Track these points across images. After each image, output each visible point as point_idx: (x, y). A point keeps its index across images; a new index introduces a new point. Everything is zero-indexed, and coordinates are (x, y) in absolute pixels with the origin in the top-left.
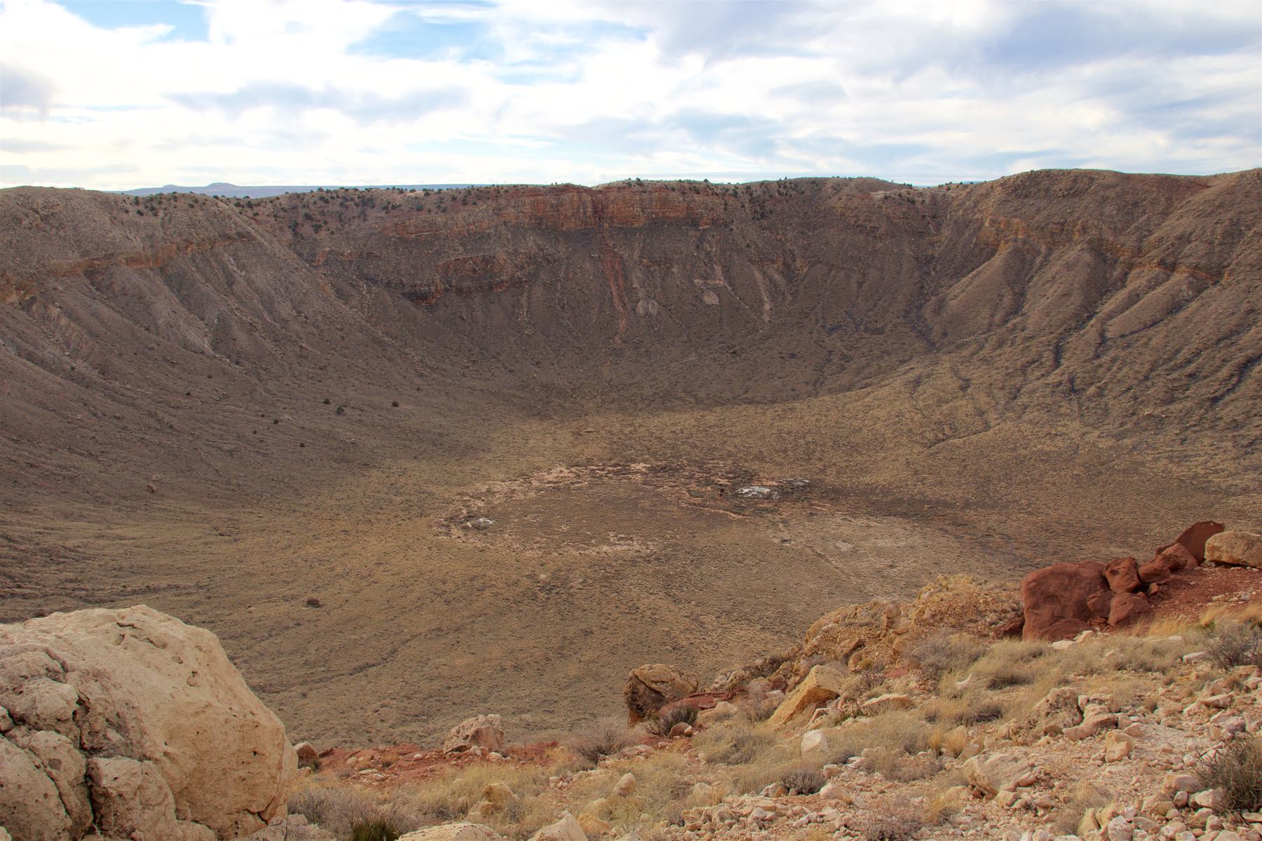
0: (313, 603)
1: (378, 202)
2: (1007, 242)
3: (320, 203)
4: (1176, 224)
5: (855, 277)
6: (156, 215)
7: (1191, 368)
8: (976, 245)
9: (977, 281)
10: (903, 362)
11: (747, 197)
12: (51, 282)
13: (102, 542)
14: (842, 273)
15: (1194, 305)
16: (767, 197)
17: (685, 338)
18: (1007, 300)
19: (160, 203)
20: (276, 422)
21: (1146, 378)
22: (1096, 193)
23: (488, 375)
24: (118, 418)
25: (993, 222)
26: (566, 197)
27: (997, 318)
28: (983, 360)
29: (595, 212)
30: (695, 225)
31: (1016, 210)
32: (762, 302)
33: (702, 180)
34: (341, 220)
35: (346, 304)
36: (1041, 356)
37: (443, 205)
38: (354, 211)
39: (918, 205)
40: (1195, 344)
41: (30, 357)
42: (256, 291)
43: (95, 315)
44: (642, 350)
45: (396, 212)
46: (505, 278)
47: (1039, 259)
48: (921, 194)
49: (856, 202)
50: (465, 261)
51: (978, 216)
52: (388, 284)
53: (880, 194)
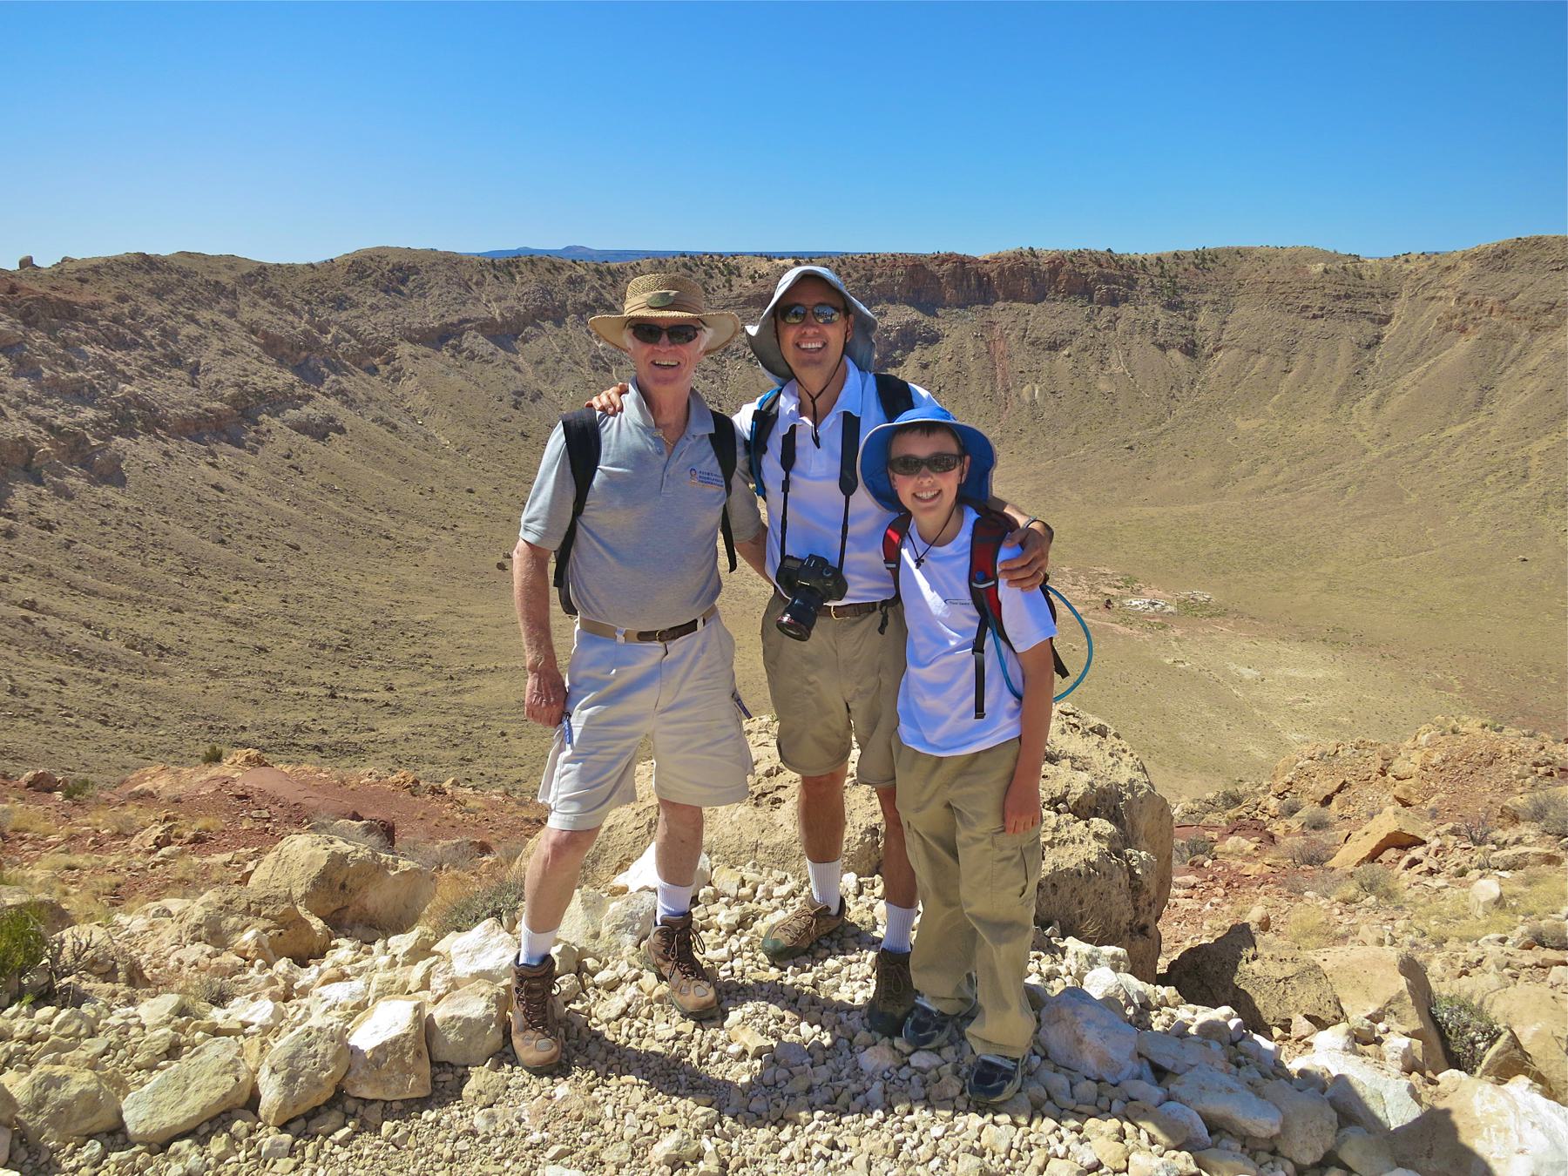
2: (1476, 326)
5: (1280, 364)
9: (1432, 373)
11: (1158, 270)
12: (404, 349)
13: (452, 618)
16: (1180, 269)
18: (1471, 395)
24: (470, 491)
33: (1103, 249)
38: (720, 280)
39: (1367, 282)
47: (1516, 348)
51: (1442, 293)
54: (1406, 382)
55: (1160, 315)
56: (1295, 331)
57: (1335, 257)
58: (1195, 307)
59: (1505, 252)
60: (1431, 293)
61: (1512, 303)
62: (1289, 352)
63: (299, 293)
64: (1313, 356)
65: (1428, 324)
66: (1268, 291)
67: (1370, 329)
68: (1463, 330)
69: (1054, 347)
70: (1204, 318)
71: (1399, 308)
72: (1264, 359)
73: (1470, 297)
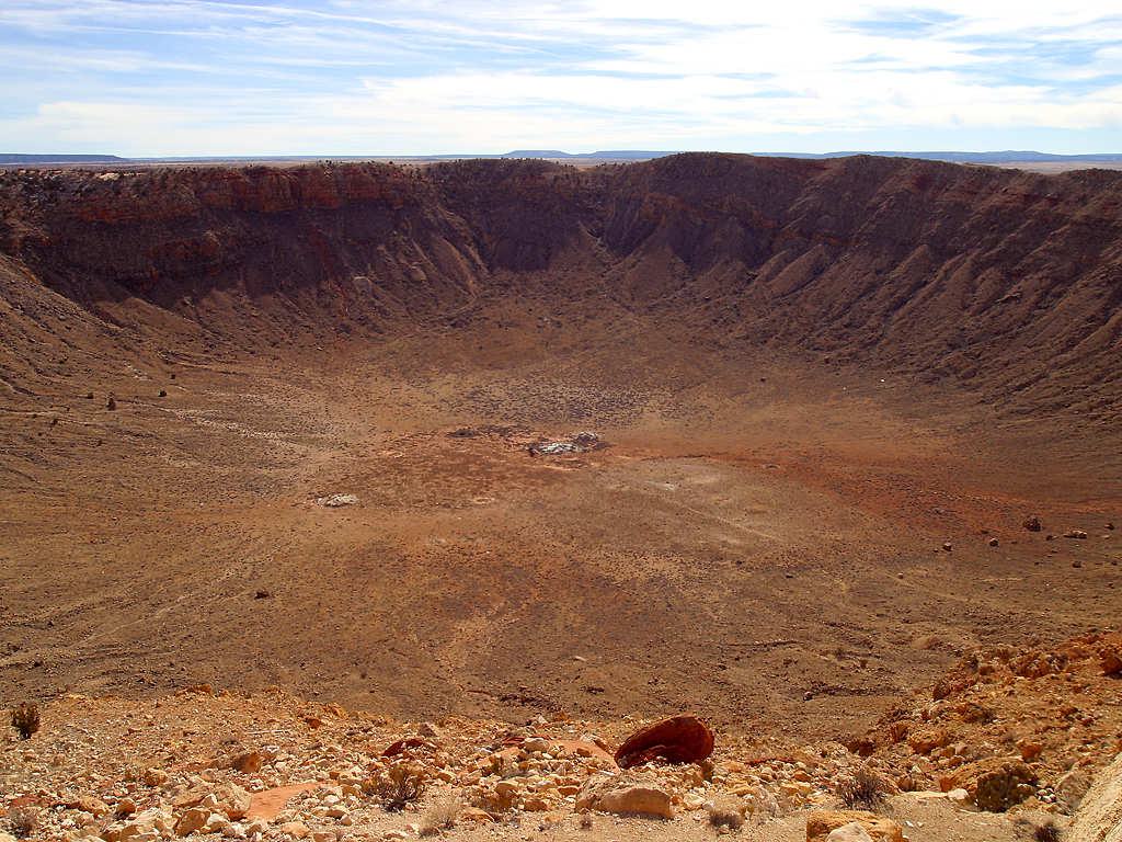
0: (261, 595)
4: (808, 199)
7: (846, 320)
8: (639, 219)
14: (529, 248)
15: (834, 268)
21: (813, 330)
23: (231, 358)
25: (652, 198)
30: (390, 206)
32: (465, 278)
40: (843, 299)
46: (218, 261)
48: (583, 175)
50: (175, 245)
52: (98, 272)
53: (550, 176)
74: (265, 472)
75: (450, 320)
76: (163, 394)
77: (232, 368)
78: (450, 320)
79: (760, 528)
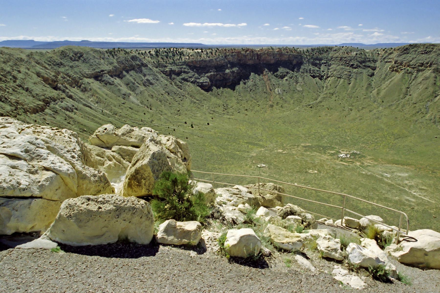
1: (185, 53)
2: (402, 70)
3: (165, 54)
6: (114, 57)
9: (392, 83)
10: (370, 111)
12: (86, 80)
17: (292, 102)
18: (404, 90)
19: (114, 52)
20: (174, 130)
22: (435, 52)
26: (248, 52)
27: (401, 96)
28: (399, 111)
29: (258, 58)
31: (404, 58)
34: (173, 60)
35: (179, 88)
36: (421, 110)
37: (208, 55)
41: (89, 107)
42: (151, 84)
43: (103, 92)
44: (280, 105)
45: (192, 57)
47: (414, 76)
49: (346, 55)
51: (389, 60)
54: (384, 86)
55: (311, 67)
56: (350, 72)
57: (357, 50)
58: (320, 65)
59: (407, 49)
60: (386, 60)
61: (411, 63)
62: (349, 77)
63: (46, 61)
64: (356, 79)
65: (387, 69)
66: (341, 60)
67: (371, 71)
68: (396, 71)
69: (282, 77)
70: (323, 67)
71: (378, 64)
72: (342, 80)
73: (399, 61)
74: (238, 153)
75: (309, 105)
76: (208, 124)
77: (232, 117)
78: (309, 105)
79: (424, 196)
